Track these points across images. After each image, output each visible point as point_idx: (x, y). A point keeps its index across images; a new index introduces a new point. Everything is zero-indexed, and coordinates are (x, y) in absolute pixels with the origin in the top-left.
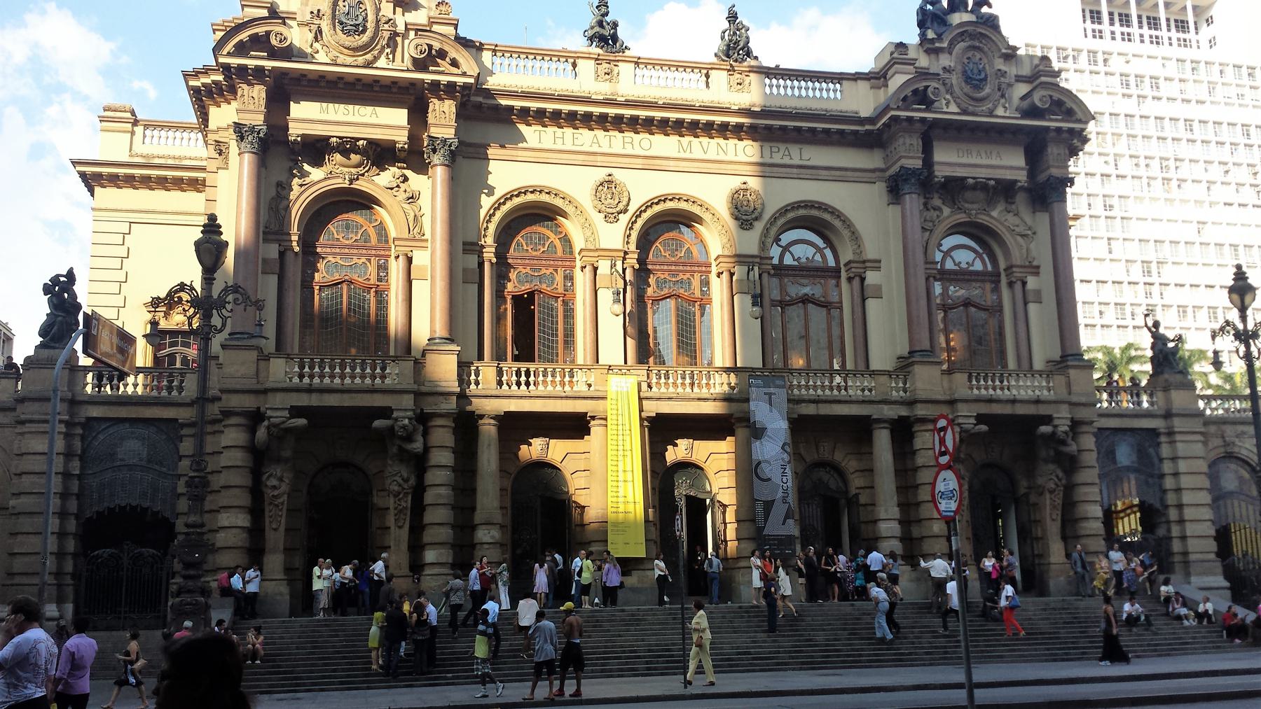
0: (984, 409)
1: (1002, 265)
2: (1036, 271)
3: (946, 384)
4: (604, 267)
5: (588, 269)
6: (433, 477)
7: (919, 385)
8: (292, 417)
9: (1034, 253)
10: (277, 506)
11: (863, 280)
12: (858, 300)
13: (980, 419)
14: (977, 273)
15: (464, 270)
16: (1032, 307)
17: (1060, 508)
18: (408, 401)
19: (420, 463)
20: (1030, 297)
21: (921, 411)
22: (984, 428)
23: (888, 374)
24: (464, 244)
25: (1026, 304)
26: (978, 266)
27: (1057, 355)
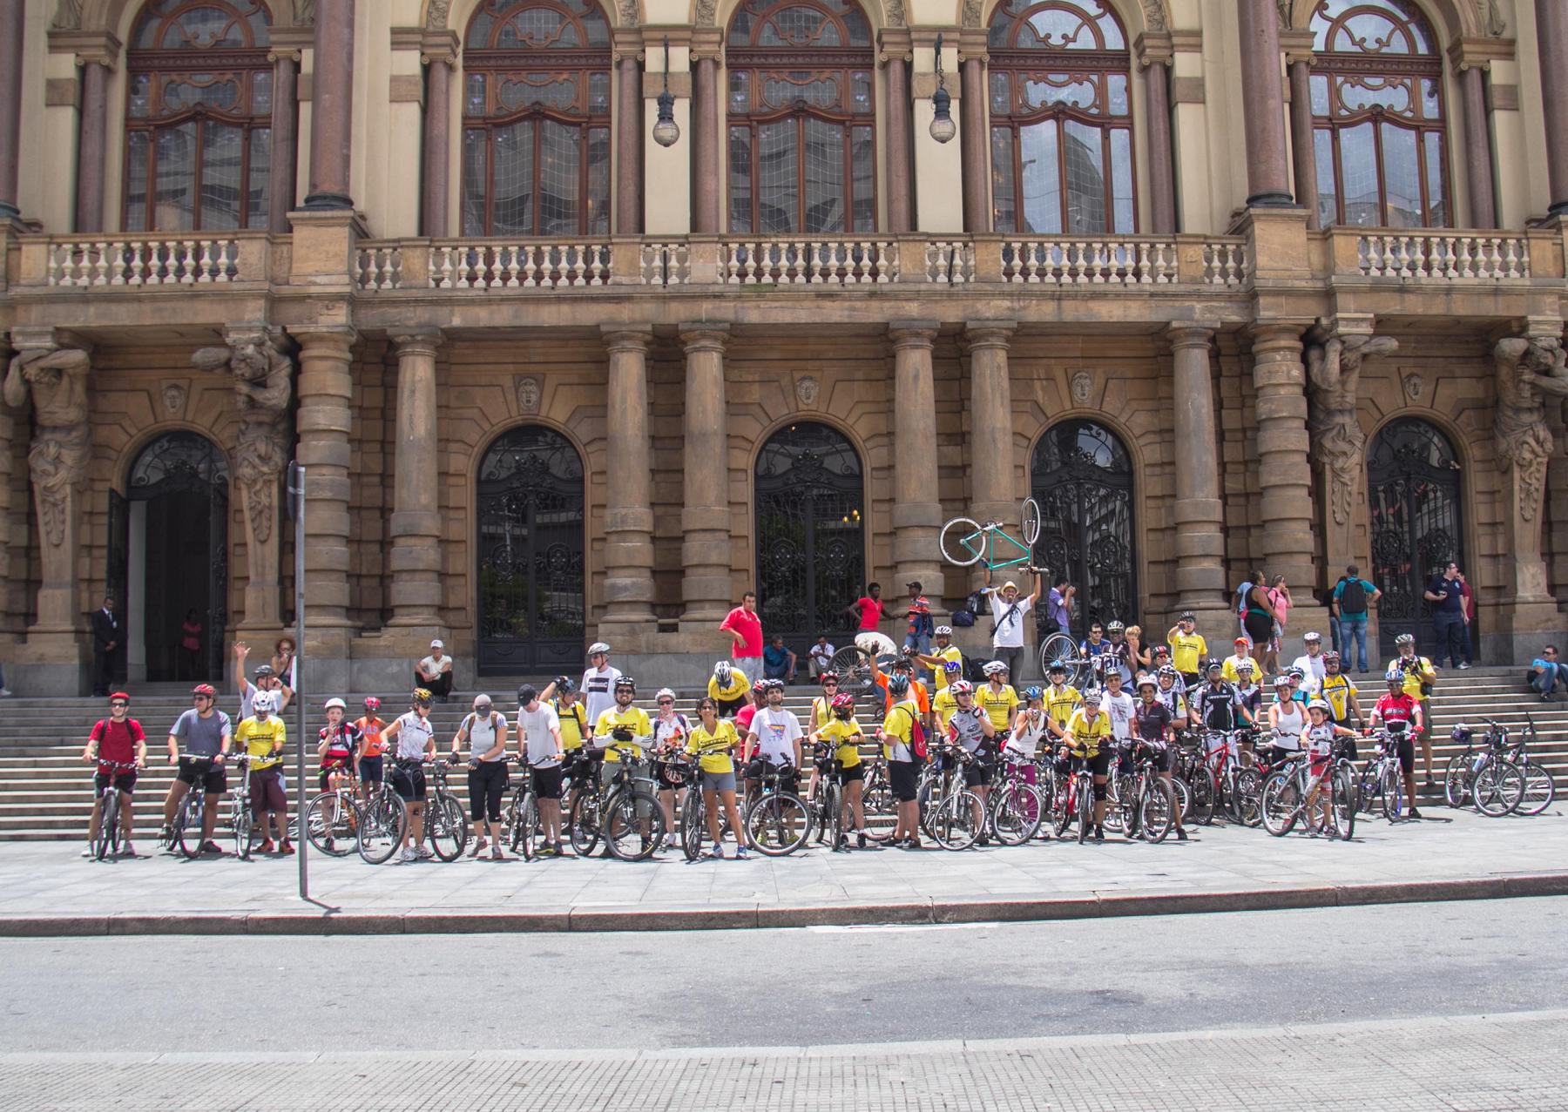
0: (1392, 306)
1: (1445, 42)
2: (1508, 50)
3: (1316, 259)
4: (654, 59)
5: (629, 65)
6: (313, 450)
7: (1262, 260)
8: (63, 346)
9: (1504, 16)
10: (55, 505)
11: (1168, 70)
12: (1159, 110)
13: (1382, 325)
14: (1396, 59)
15: (394, 79)
16: (1501, 119)
17: (1540, 496)
18: (255, 312)
19: (288, 426)
20: (1497, 100)
21: (1268, 311)
22: (1392, 344)
23: (1204, 239)
24: (395, 31)
25: (1488, 112)
26: (1399, 46)
27: (1541, 202)
